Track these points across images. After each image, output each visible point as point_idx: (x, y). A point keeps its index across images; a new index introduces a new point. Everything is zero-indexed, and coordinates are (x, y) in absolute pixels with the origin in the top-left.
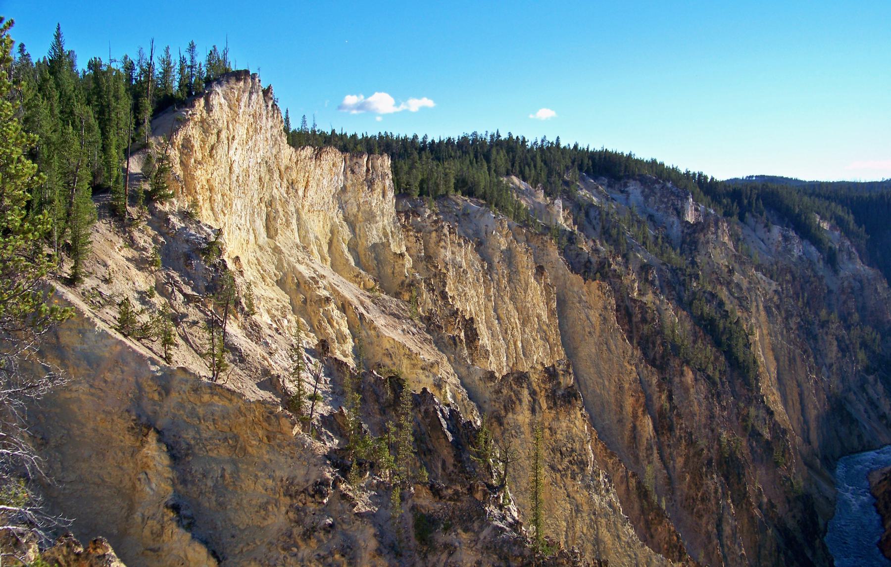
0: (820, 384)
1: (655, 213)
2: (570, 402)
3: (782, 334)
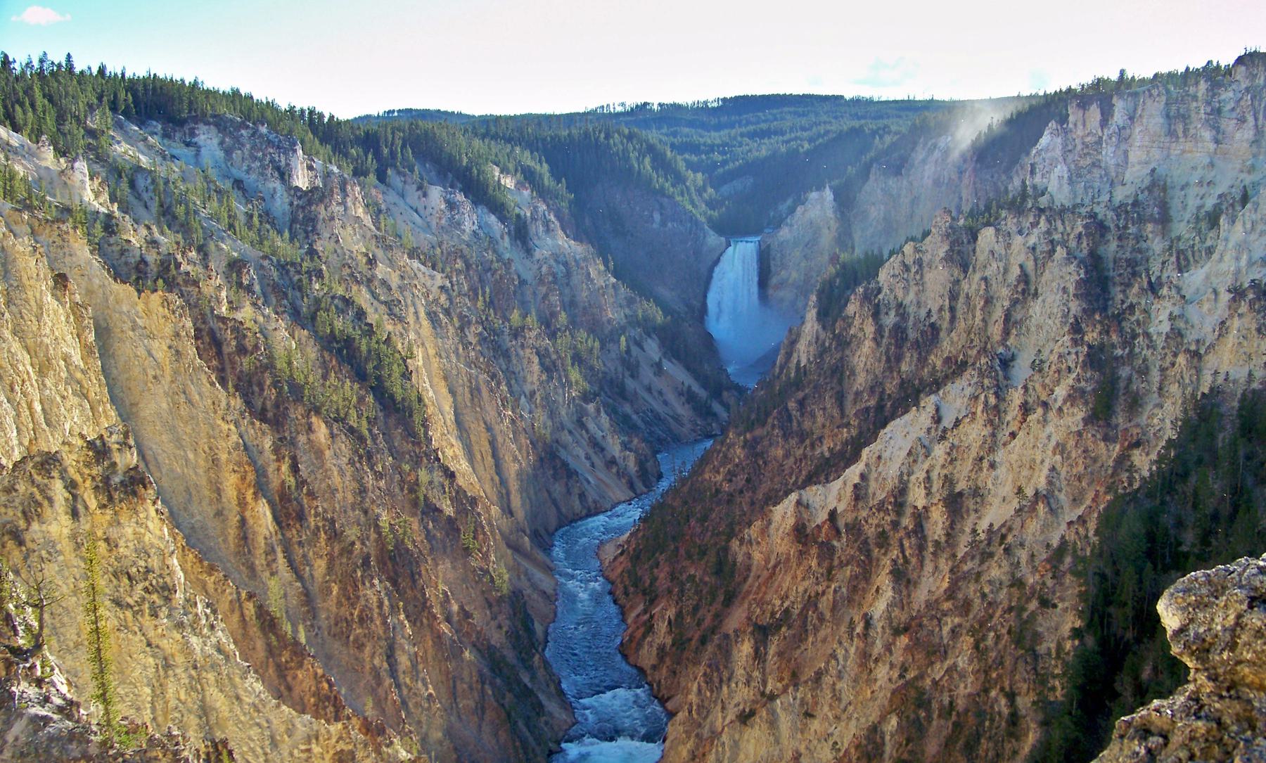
0: (519, 423)
1: (243, 176)
2: (135, 493)
3: (456, 352)
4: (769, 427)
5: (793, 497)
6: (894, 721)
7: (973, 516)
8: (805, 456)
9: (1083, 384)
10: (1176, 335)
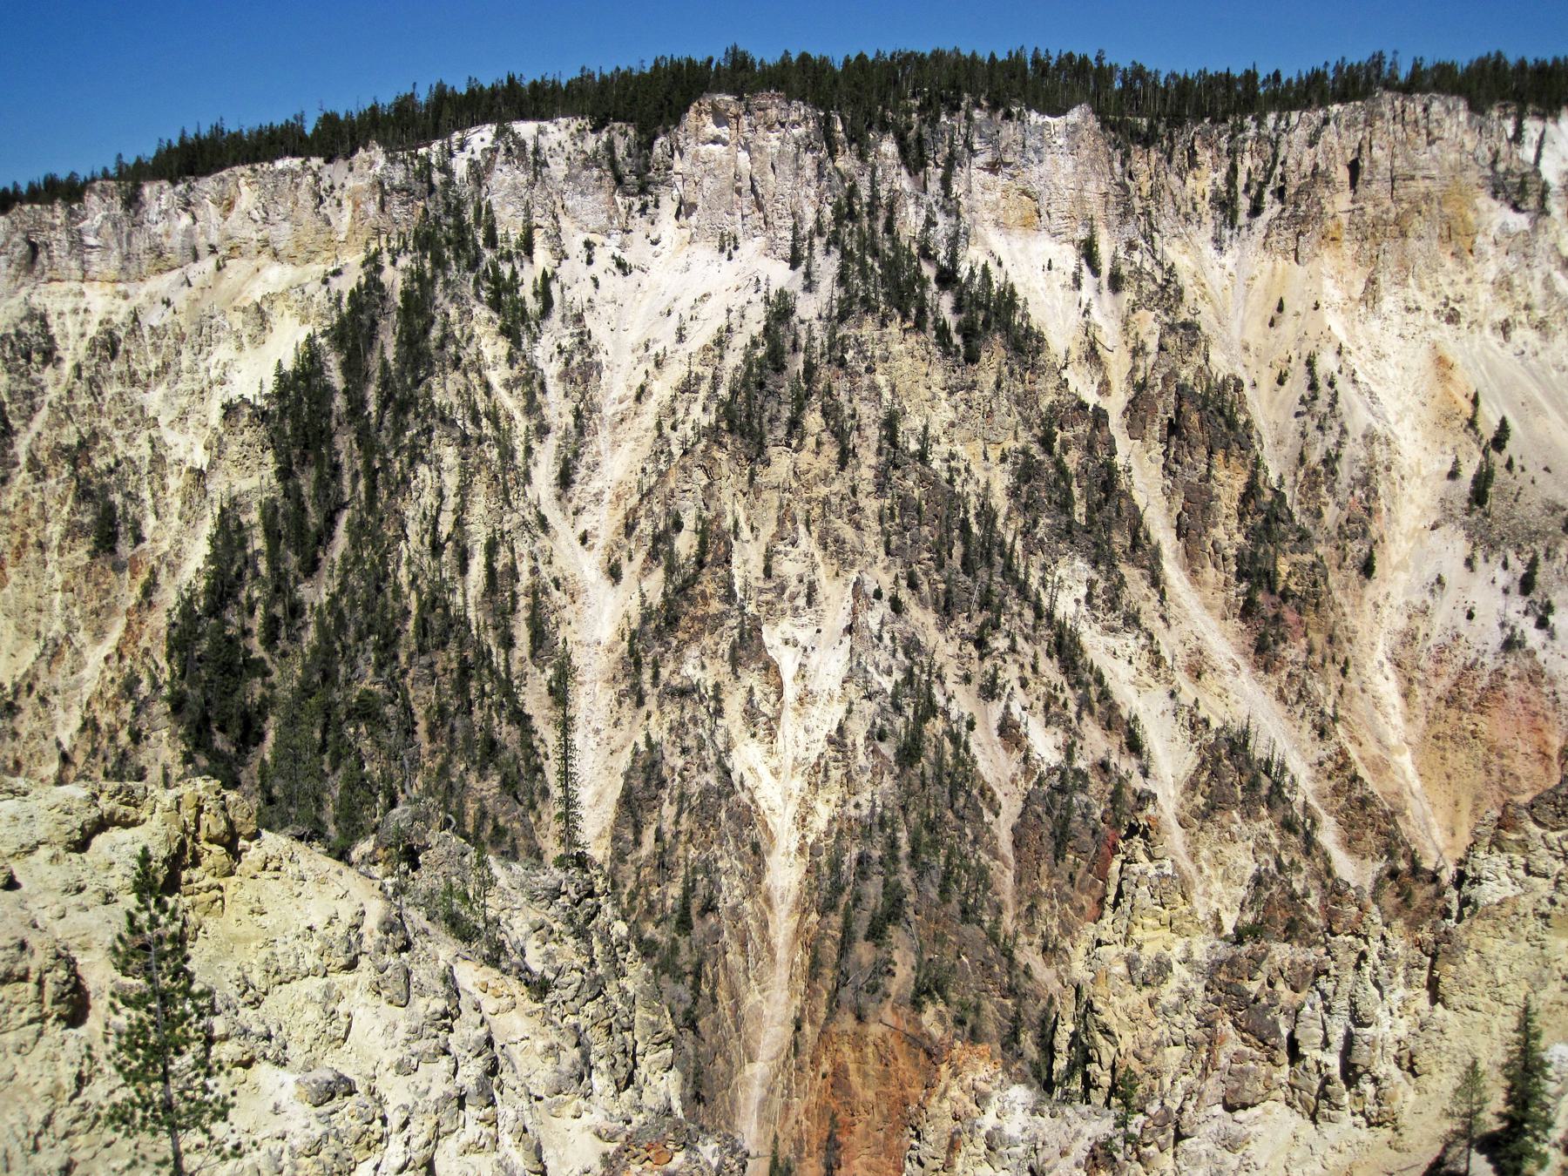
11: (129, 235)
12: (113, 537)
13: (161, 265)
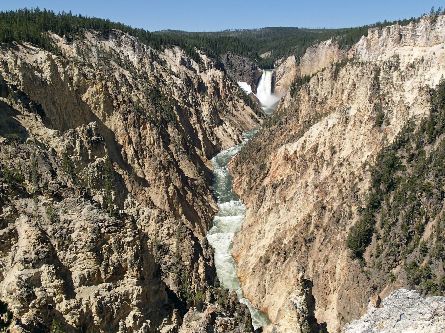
4: (276, 126)
5: (284, 146)
6: (315, 212)
7: (338, 154)
8: (287, 135)
9: (372, 115)
10: (401, 101)
11: (430, 32)
12: (382, 123)
13: (437, 42)
